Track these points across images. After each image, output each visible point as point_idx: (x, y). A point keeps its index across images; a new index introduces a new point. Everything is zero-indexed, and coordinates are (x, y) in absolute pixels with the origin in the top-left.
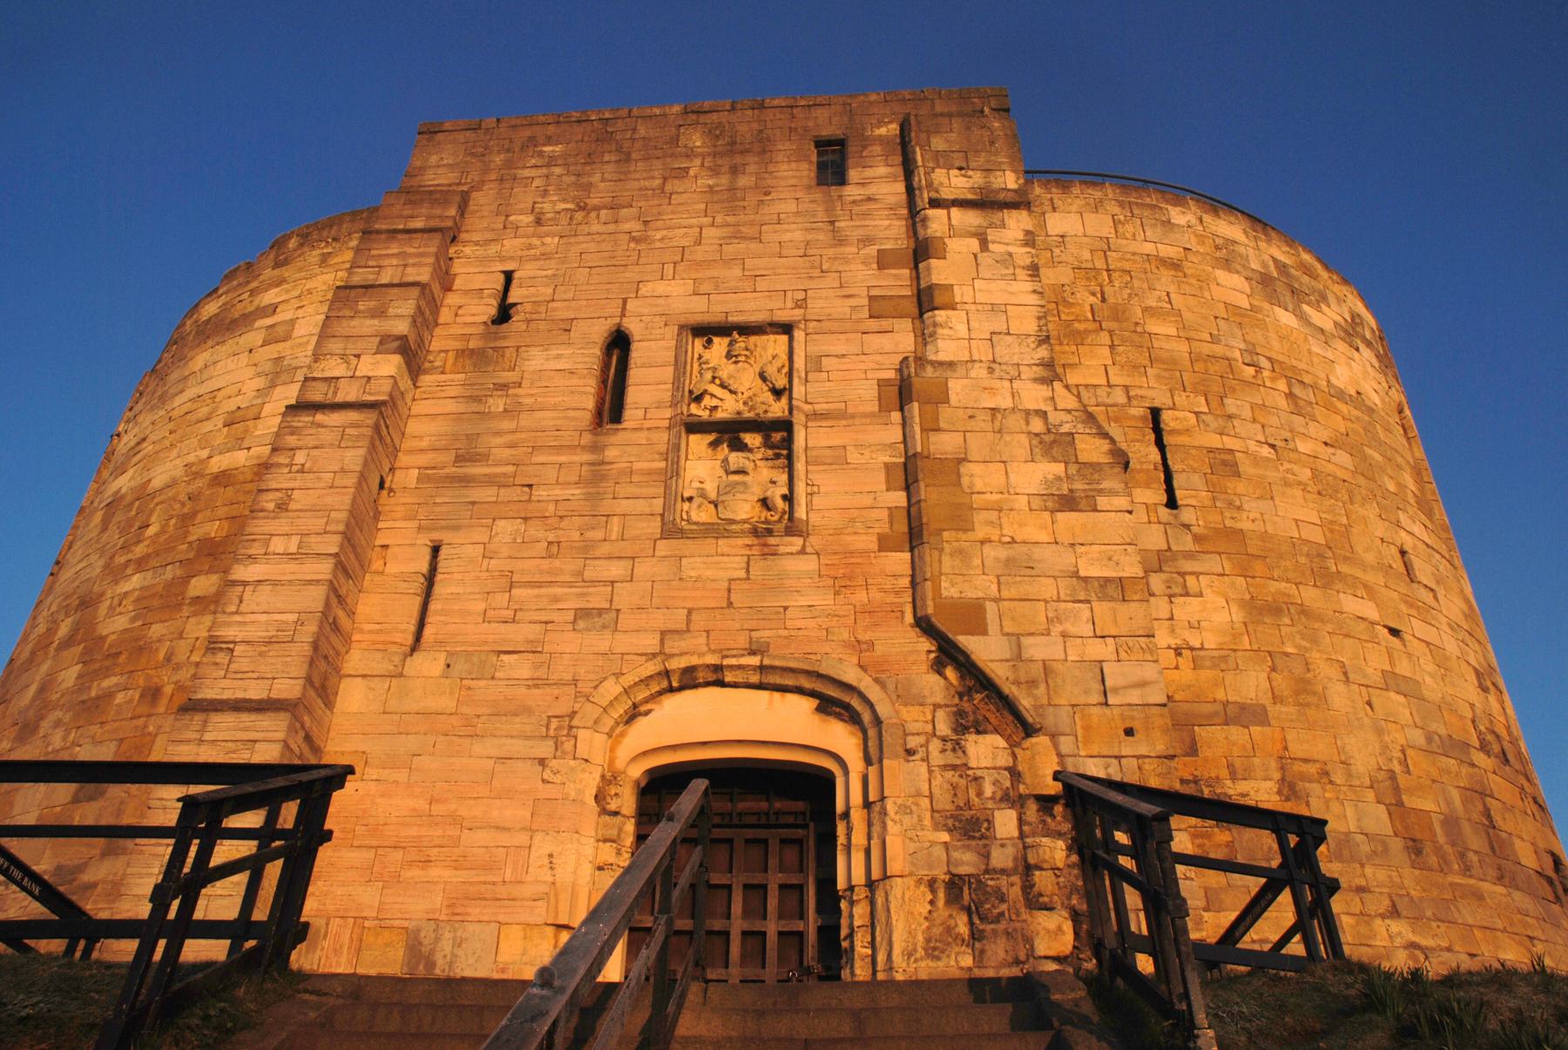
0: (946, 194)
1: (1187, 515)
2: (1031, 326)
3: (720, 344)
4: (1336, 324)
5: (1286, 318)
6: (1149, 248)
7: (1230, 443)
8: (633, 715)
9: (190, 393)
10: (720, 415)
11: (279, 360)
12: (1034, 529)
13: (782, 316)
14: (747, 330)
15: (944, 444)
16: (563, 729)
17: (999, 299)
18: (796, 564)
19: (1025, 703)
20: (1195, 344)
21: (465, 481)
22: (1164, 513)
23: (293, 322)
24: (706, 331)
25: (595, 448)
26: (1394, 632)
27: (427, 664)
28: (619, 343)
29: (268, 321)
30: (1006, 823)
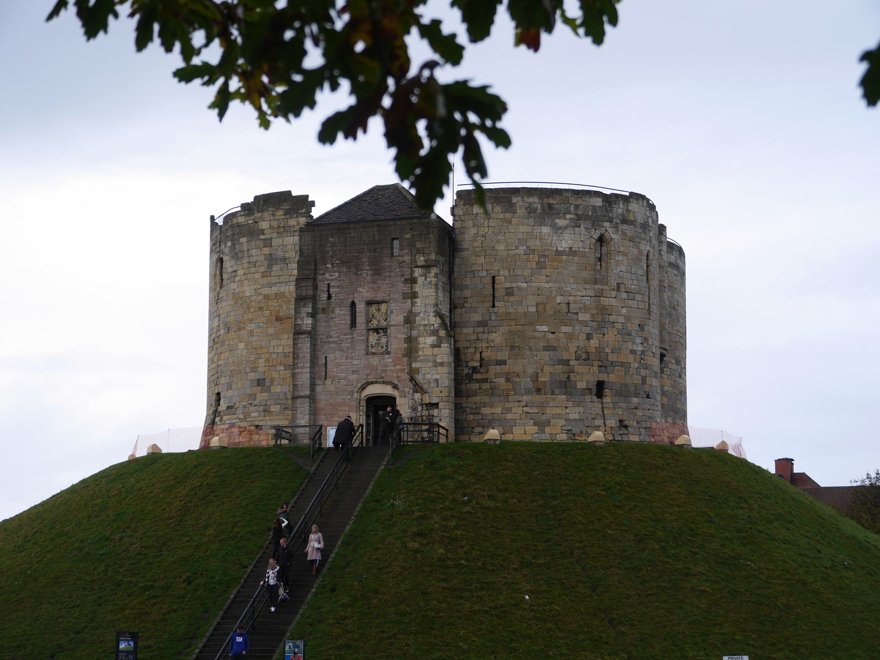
0: (419, 264)
1: (496, 310)
2: (433, 302)
3: (374, 307)
4: (570, 219)
5: (545, 230)
6: (502, 216)
7: (513, 285)
8: (364, 389)
9: (246, 260)
10: (374, 326)
11: (270, 255)
12: (428, 352)
13: (387, 298)
14: (379, 303)
15: (415, 333)
16: (352, 393)
17: (428, 294)
18: (388, 359)
19: (425, 387)
20: (510, 252)
21: (330, 342)
22: (491, 310)
23: (271, 239)
24: (369, 303)
25: (352, 334)
26: (553, 333)
27: (329, 382)
28: (353, 304)
29: (262, 237)
30: (420, 408)
